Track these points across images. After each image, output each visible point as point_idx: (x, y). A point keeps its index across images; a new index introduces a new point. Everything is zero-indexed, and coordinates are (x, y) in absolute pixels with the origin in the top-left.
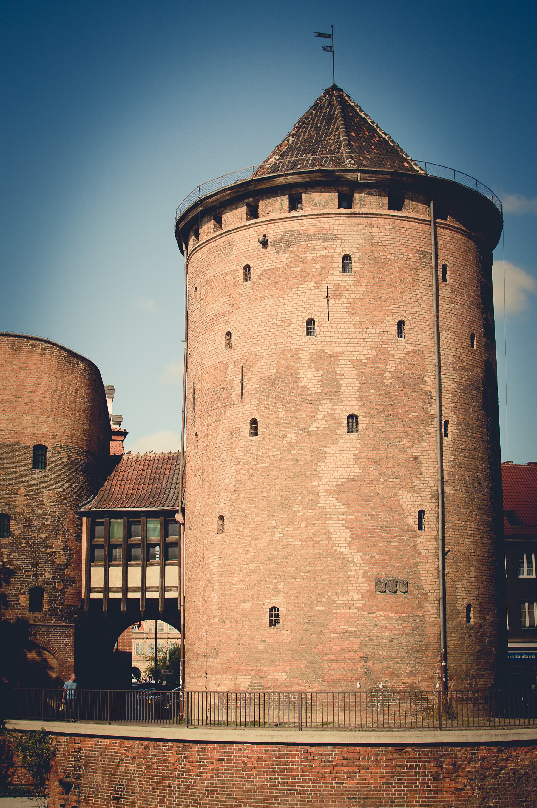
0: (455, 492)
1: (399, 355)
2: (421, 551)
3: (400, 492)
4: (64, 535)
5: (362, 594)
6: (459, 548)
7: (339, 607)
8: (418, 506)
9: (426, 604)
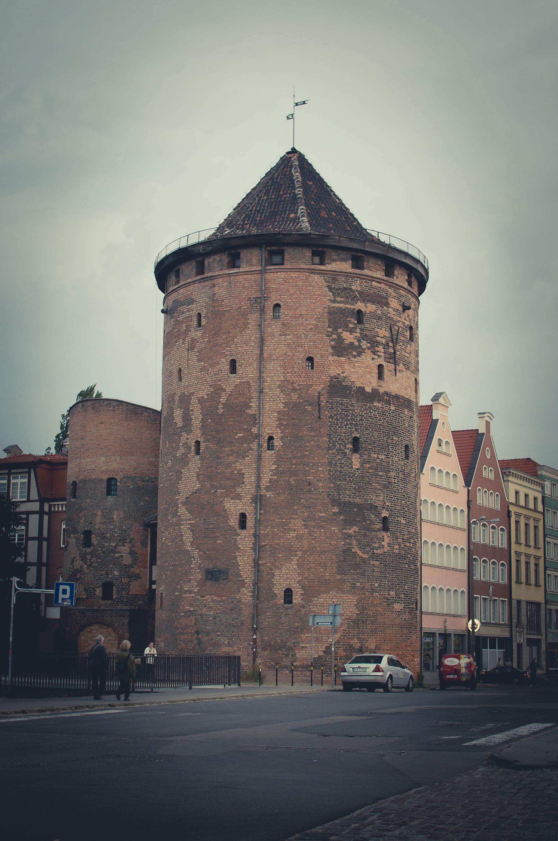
0: (276, 496)
1: (229, 389)
2: (239, 546)
3: (226, 499)
4: (130, 542)
5: (198, 582)
6: (279, 541)
7: (186, 592)
8: (239, 509)
9: (243, 589)
